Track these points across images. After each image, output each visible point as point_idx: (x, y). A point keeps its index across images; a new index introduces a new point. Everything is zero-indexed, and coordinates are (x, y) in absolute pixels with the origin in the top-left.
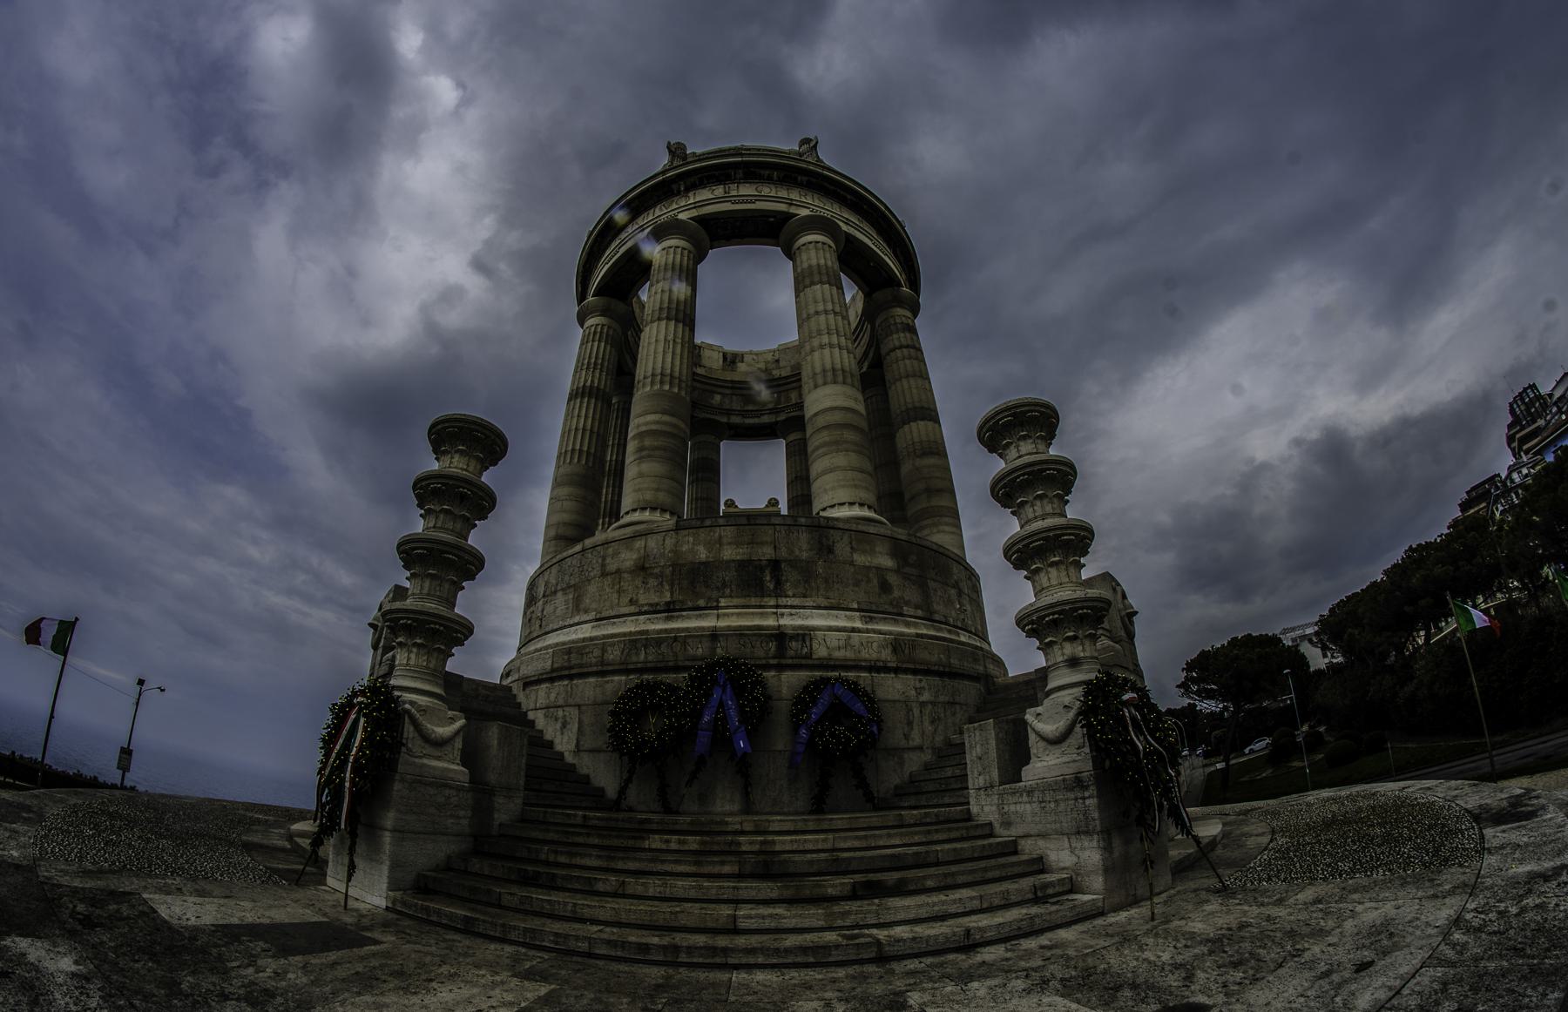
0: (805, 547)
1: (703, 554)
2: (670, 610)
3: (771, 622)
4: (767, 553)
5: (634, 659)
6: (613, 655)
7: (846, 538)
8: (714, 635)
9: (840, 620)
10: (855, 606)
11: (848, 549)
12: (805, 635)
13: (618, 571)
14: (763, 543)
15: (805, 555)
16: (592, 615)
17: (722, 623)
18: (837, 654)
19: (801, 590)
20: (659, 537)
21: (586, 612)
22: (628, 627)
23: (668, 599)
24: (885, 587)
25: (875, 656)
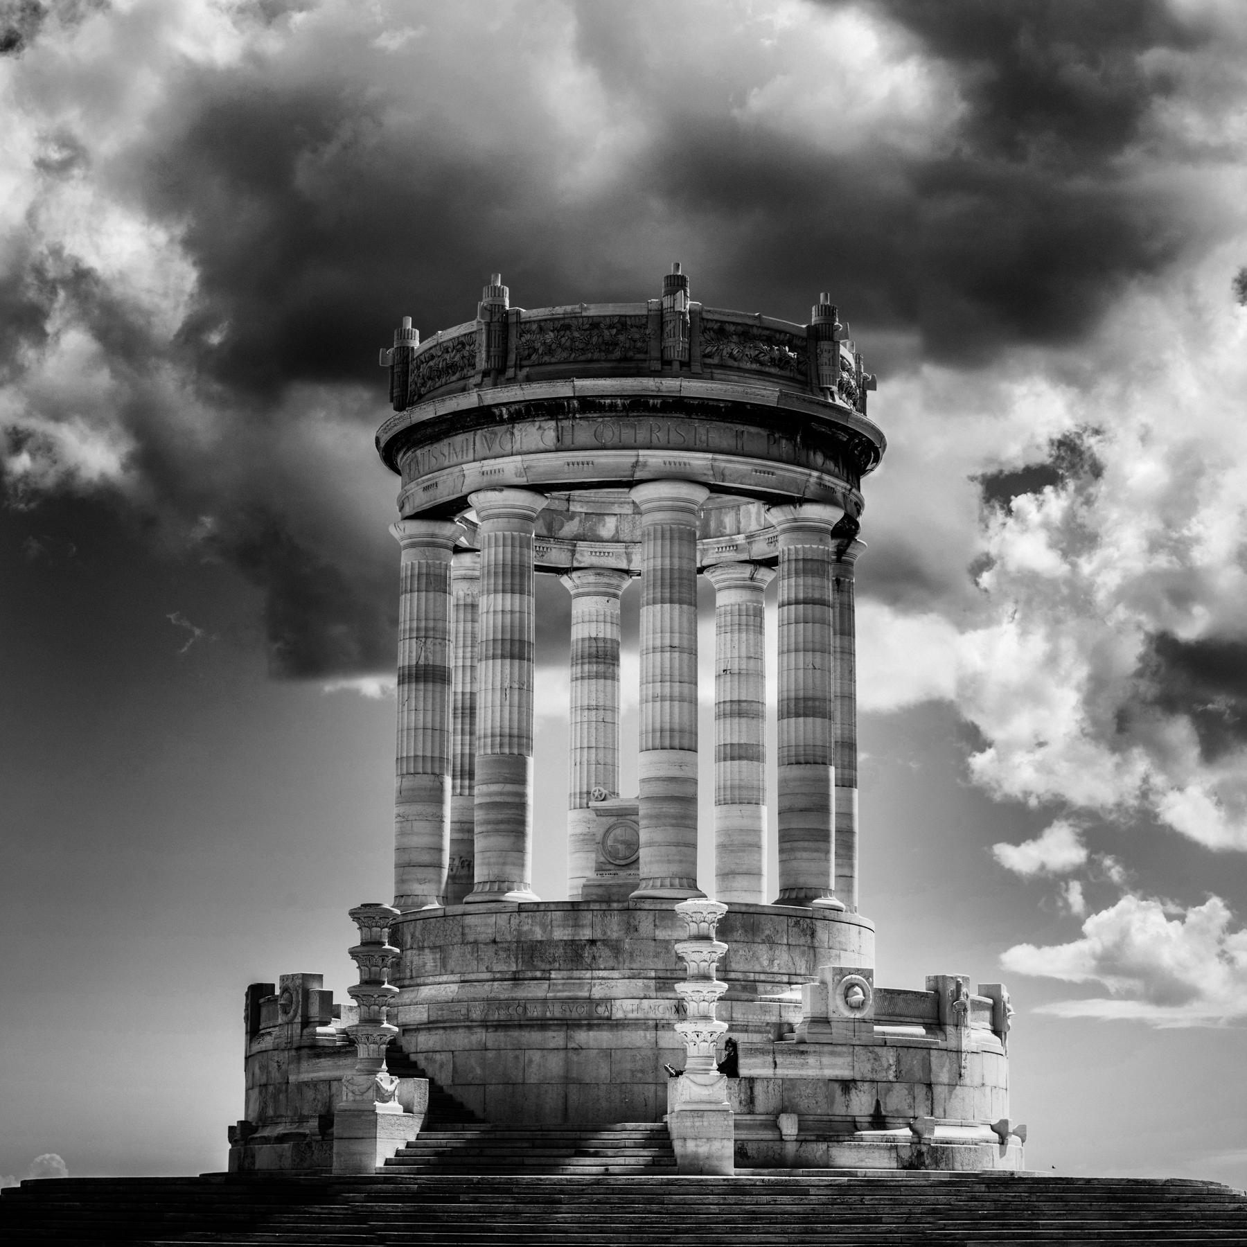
0: (615, 928)
1: (538, 934)
2: (516, 979)
4: (586, 934)
5: (491, 1018)
7: (651, 918)
10: (653, 974)
11: (652, 926)
13: (476, 942)
14: (583, 926)
15: (615, 936)
16: (456, 978)
18: (630, 1016)
19: (611, 963)
20: (505, 916)
21: (452, 973)
22: (484, 990)
23: (514, 969)
25: (660, 1016)
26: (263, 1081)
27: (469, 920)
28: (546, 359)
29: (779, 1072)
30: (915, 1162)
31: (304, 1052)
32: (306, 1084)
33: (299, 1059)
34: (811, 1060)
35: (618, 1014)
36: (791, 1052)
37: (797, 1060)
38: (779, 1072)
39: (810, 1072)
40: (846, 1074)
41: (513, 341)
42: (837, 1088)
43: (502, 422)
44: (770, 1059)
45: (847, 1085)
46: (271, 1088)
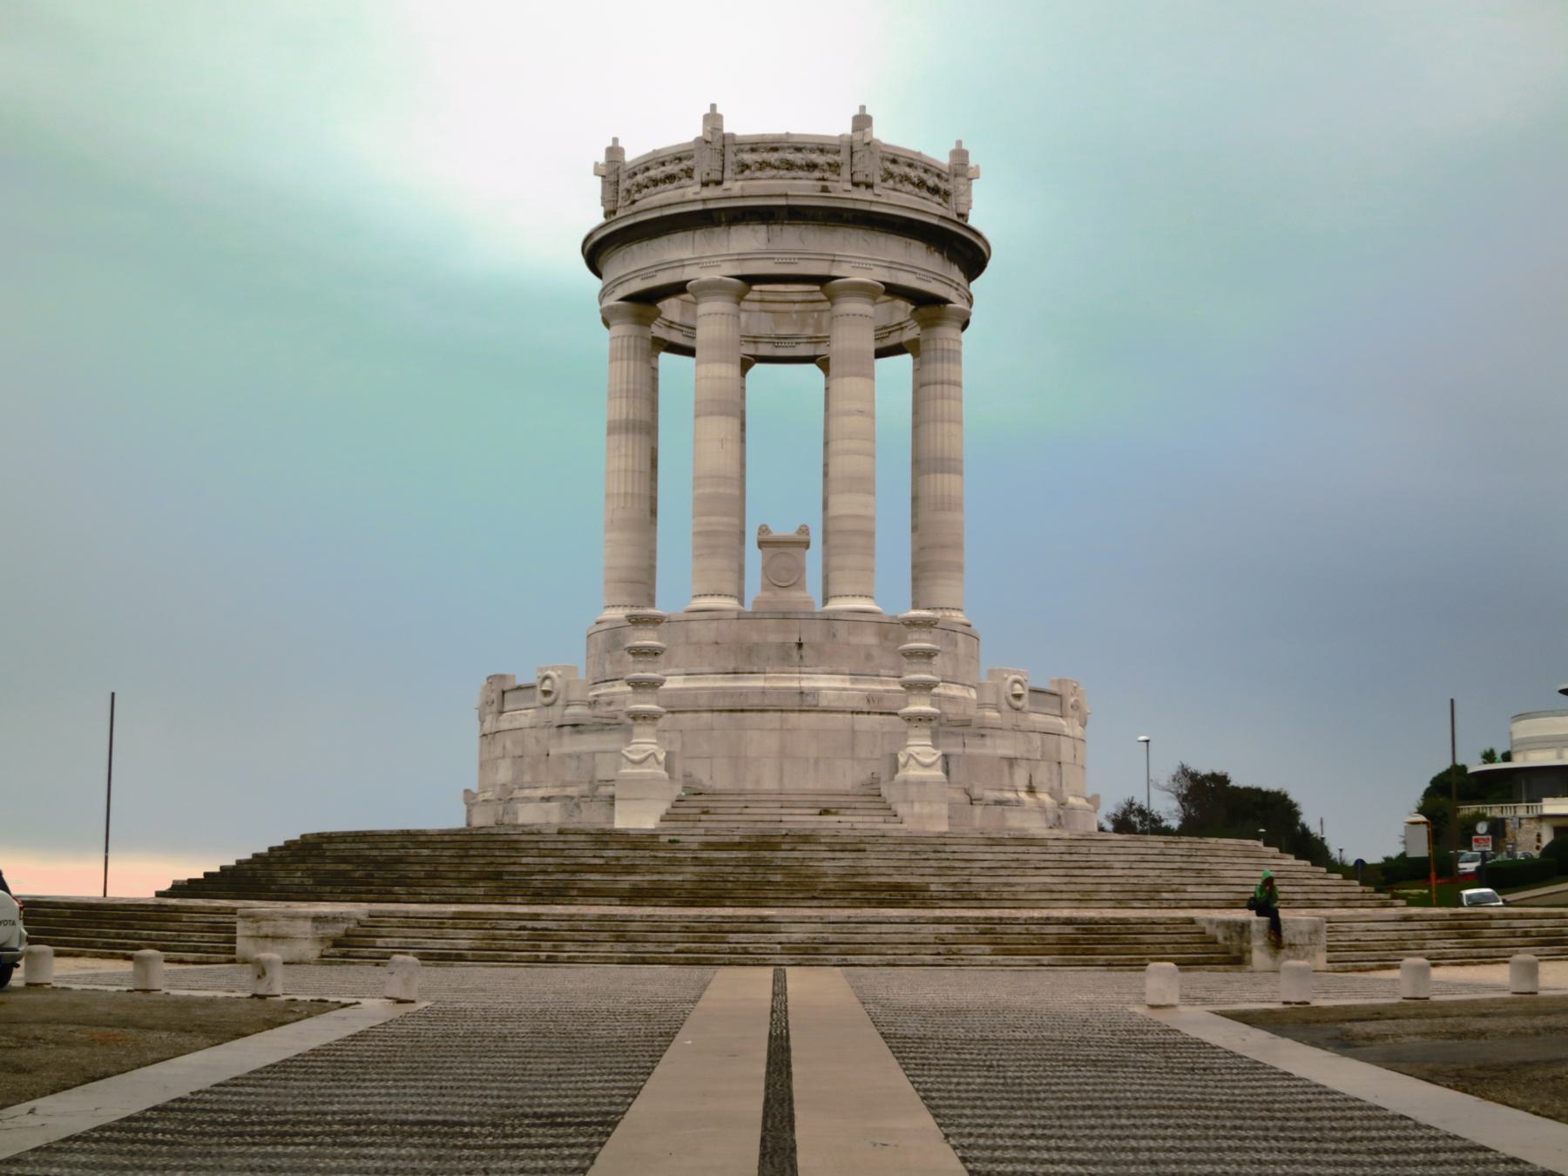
1: (755, 638)
3: (795, 684)
6: (703, 702)
8: (763, 691)
9: (836, 682)
12: (815, 692)
13: (699, 643)
16: (683, 670)
17: (768, 685)
24: (869, 657)
26: (518, 752)
27: (693, 625)
28: (758, 174)
29: (968, 750)
30: (1058, 822)
31: (567, 729)
32: (570, 756)
33: (560, 736)
34: (988, 741)
35: (823, 703)
36: (975, 735)
37: (978, 741)
38: (968, 750)
39: (987, 751)
40: (1010, 753)
41: (730, 158)
42: (1005, 765)
43: (719, 224)
44: (960, 740)
45: (1012, 761)
46: (527, 760)
